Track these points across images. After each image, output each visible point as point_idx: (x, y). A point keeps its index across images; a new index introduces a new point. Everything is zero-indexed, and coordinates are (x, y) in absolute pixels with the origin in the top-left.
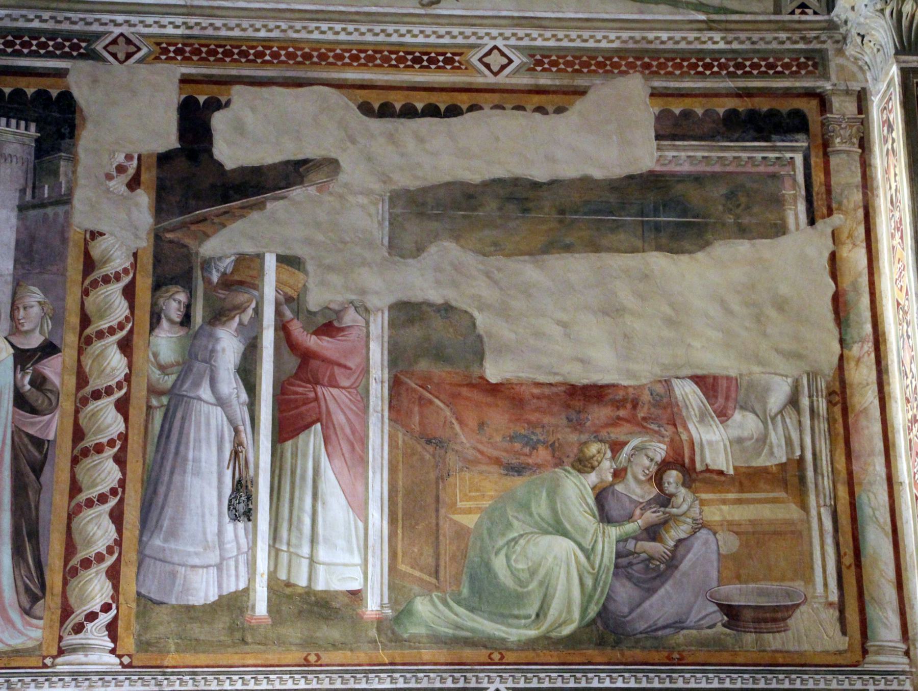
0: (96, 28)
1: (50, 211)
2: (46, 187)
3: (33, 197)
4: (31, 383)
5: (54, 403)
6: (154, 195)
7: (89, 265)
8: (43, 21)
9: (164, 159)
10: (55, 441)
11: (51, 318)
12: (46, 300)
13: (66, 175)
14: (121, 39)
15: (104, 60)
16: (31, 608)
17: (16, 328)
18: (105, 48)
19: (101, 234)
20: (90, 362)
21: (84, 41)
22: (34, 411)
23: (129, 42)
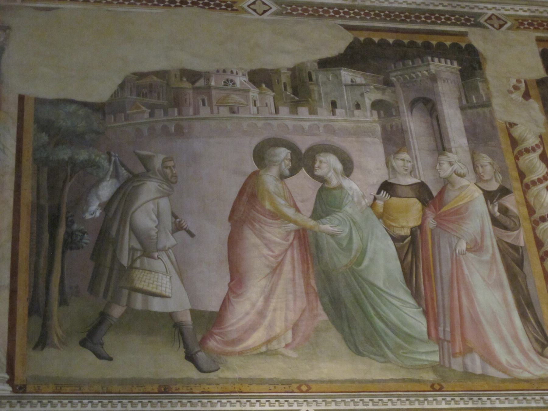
0: (476, 10)
1: (480, 110)
2: (474, 97)
3: (467, 102)
4: (499, 211)
5: (518, 224)
6: (541, 102)
7: (514, 142)
8: (444, 6)
9: (540, 82)
10: (525, 246)
11: (500, 173)
12: (494, 162)
13: (484, 90)
14: (493, 17)
15: (488, 28)
16: (542, 351)
17: (479, 179)
18: (486, 21)
19: (516, 125)
20: (532, 199)
21: (472, 17)
22: (506, 228)
23: (498, 18)
